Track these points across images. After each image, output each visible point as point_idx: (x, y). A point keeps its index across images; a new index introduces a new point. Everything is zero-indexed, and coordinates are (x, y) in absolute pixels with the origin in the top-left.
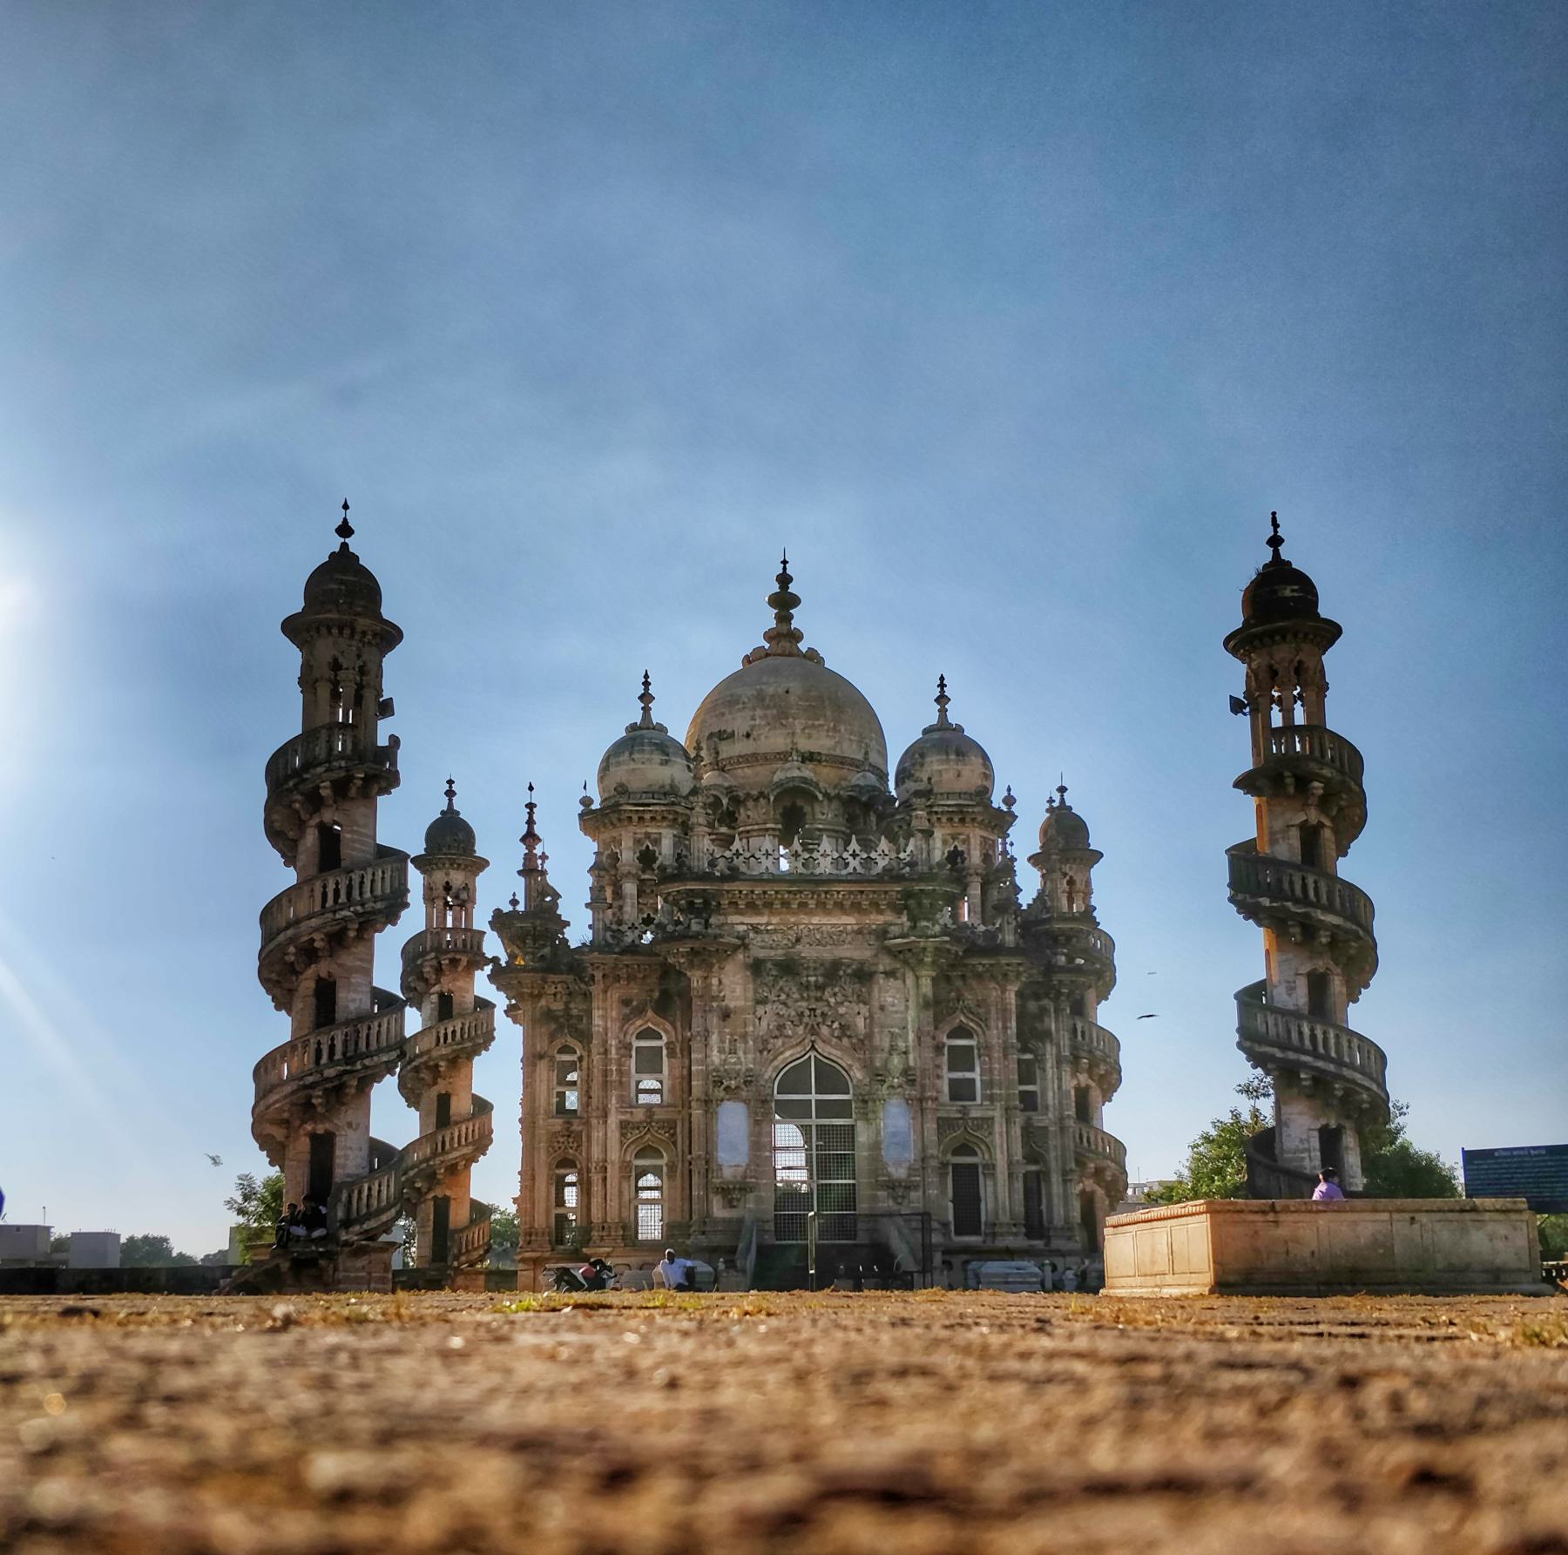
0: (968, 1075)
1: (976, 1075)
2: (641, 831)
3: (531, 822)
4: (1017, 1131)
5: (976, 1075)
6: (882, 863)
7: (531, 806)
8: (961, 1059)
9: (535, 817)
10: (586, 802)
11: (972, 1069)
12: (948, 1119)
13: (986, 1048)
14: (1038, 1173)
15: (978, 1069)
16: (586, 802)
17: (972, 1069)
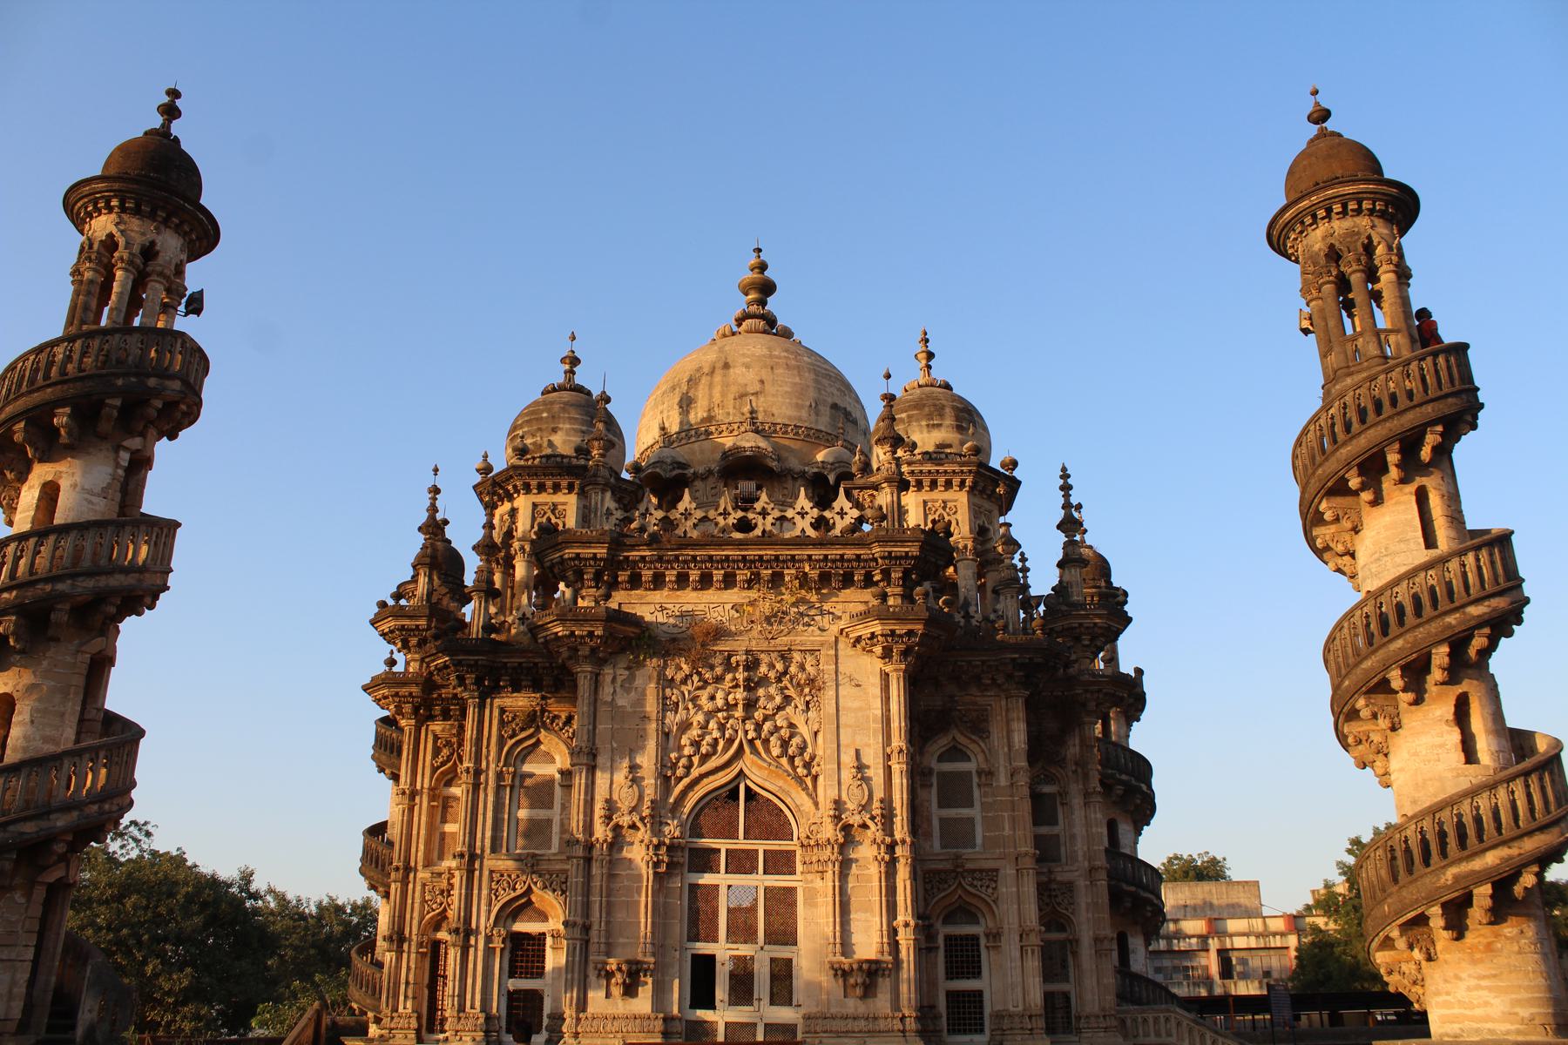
0: (964, 812)
1: (975, 812)
2: (543, 498)
3: (433, 509)
4: (1030, 888)
5: (975, 812)
6: (840, 525)
7: (435, 491)
8: (955, 791)
9: (438, 504)
10: (486, 469)
11: (972, 806)
12: (939, 872)
13: (988, 774)
14: (1063, 945)
15: (977, 804)
16: (486, 469)
17: (972, 806)
